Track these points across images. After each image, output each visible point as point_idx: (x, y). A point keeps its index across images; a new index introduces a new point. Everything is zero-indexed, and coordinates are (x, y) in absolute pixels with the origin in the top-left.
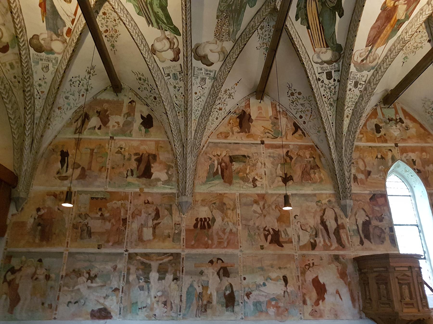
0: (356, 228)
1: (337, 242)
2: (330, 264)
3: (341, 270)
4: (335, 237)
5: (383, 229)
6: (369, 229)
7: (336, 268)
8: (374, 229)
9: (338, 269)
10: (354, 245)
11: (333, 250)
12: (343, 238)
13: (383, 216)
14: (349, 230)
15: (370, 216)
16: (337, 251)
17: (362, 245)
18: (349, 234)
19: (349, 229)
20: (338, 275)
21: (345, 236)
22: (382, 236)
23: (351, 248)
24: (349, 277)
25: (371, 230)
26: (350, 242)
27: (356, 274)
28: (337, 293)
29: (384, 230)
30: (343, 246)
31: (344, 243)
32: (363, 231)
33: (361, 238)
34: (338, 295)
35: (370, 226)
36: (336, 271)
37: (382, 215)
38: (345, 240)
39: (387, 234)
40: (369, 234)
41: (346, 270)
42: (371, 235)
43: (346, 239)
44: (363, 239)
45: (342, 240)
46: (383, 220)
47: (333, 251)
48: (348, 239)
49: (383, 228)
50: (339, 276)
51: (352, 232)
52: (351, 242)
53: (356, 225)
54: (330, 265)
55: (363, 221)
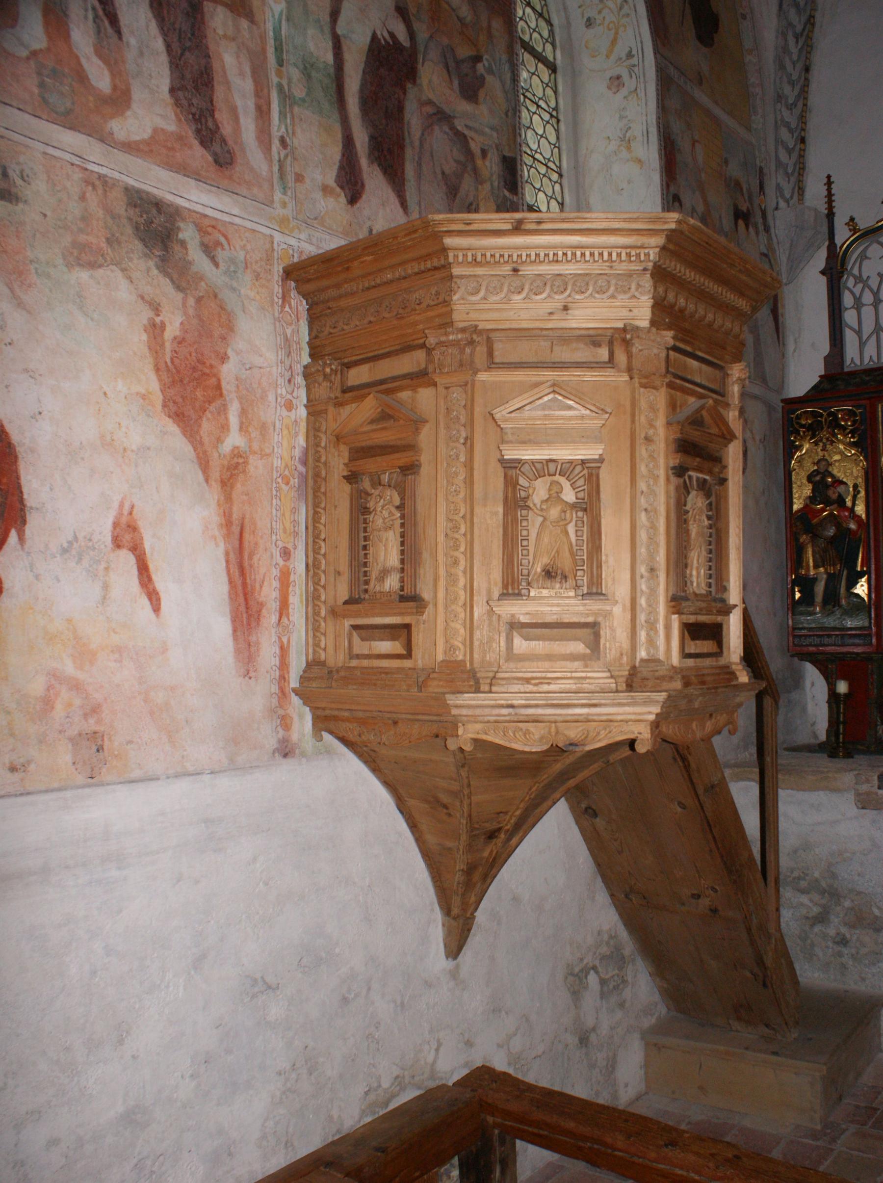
0: (330, 58)
1: (172, 91)
2: (92, 265)
3: (180, 341)
4: (159, 44)
5: (475, 147)
6: (401, 109)
7: (146, 314)
8: (427, 128)
9: (155, 330)
10: (299, 178)
11: (129, 147)
12: (227, 83)
13: (480, 67)
14: (279, 49)
15: (416, 26)
16: (164, 174)
17: (353, 199)
18: (275, 80)
19: (277, 38)
20: (154, 385)
21: (242, 74)
22: (462, 192)
23: (278, 196)
24: (234, 420)
25: (413, 118)
26: (276, 144)
27: (289, 406)
28: (117, 543)
29: (479, 162)
30: (216, 147)
31: (227, 130)
32: (368, 102)
33: (348, 142)
34: (126, 560)
35: (412, 92)
36: (139, 339)
37: (478, 59)
38: (239, 103)
39: (487, 186)
40: (402, 147)
41: (224, 358)
42: (409, 153)
43: (251, 103)
44: (364, 162)
45: (219, 93)
46: (481, 94)
47: (136, 163)
48: (262, 112)
49: (472, 145)
50: (158, 399)
51: (295, 73)
52: (283, 141)
53: (327, 29)
54: (84, 275)
55: (374, 37)
